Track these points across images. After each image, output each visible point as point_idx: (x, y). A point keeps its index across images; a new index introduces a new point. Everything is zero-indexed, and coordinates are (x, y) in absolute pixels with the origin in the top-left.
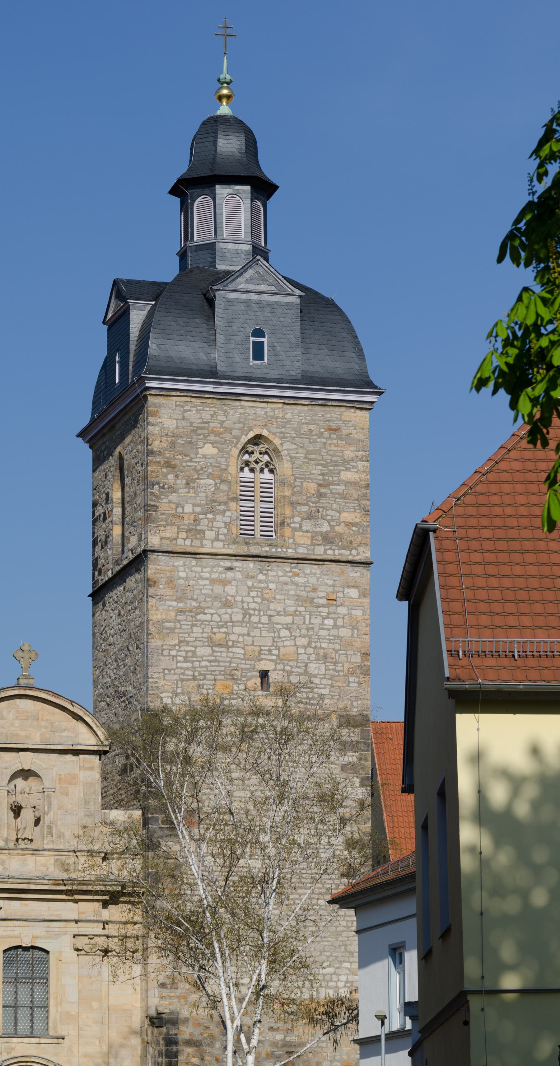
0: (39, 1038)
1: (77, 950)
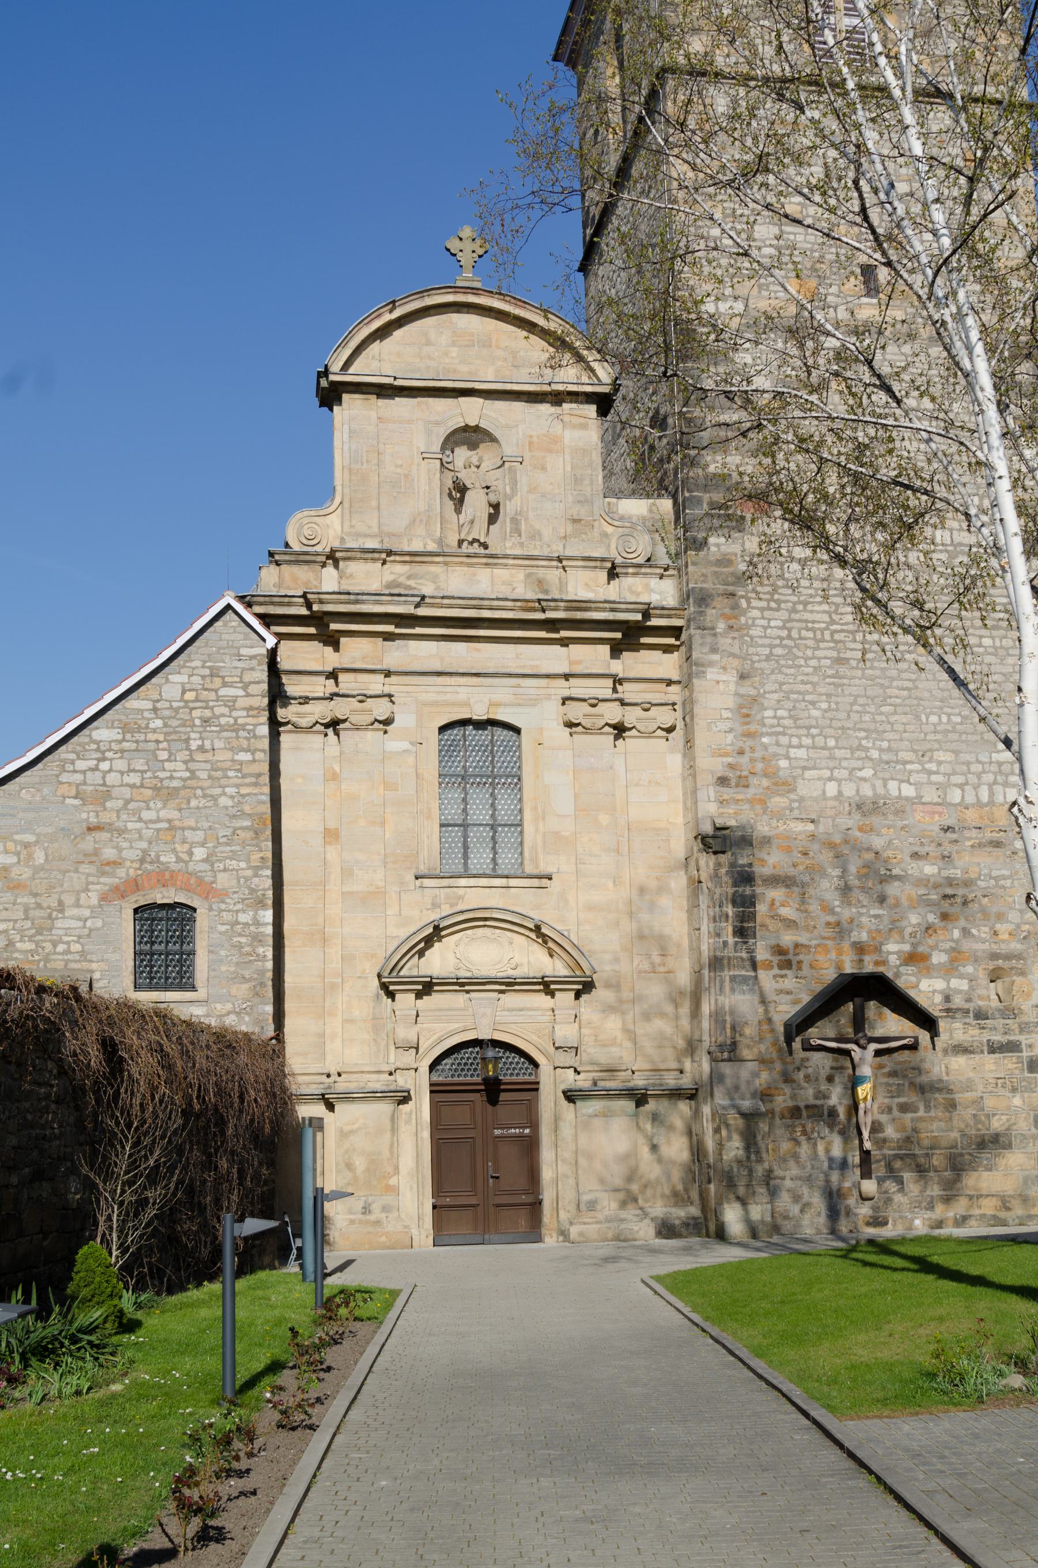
0: (507, 877)
1: (570, 725)
